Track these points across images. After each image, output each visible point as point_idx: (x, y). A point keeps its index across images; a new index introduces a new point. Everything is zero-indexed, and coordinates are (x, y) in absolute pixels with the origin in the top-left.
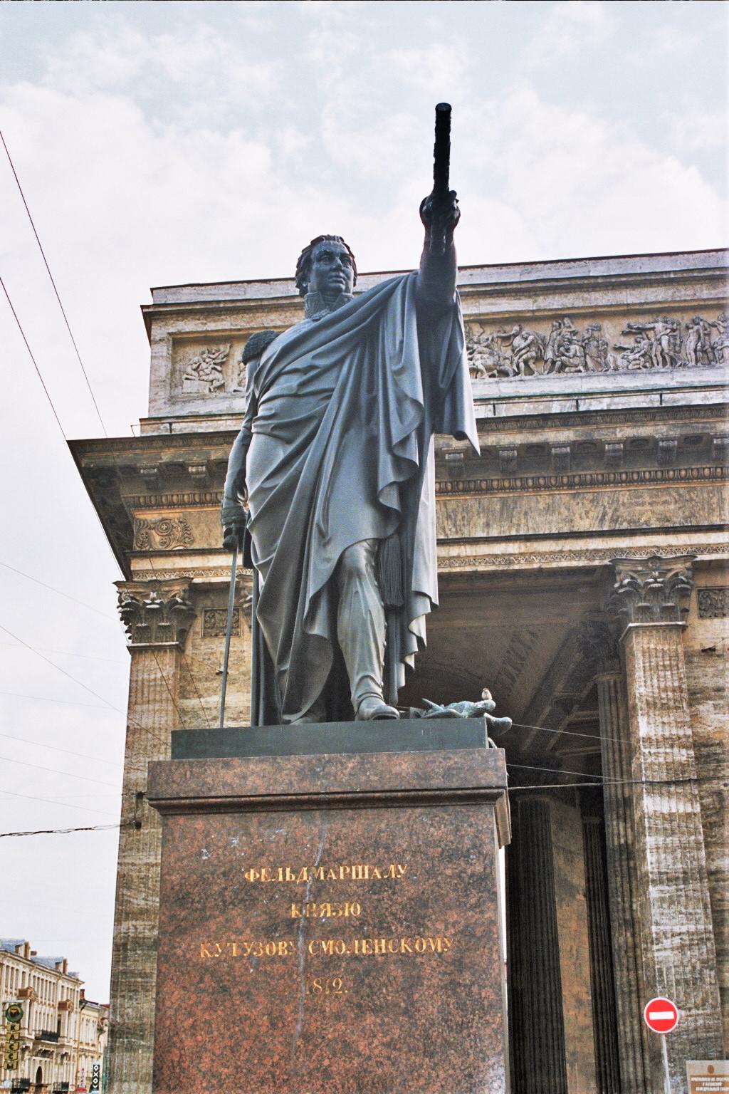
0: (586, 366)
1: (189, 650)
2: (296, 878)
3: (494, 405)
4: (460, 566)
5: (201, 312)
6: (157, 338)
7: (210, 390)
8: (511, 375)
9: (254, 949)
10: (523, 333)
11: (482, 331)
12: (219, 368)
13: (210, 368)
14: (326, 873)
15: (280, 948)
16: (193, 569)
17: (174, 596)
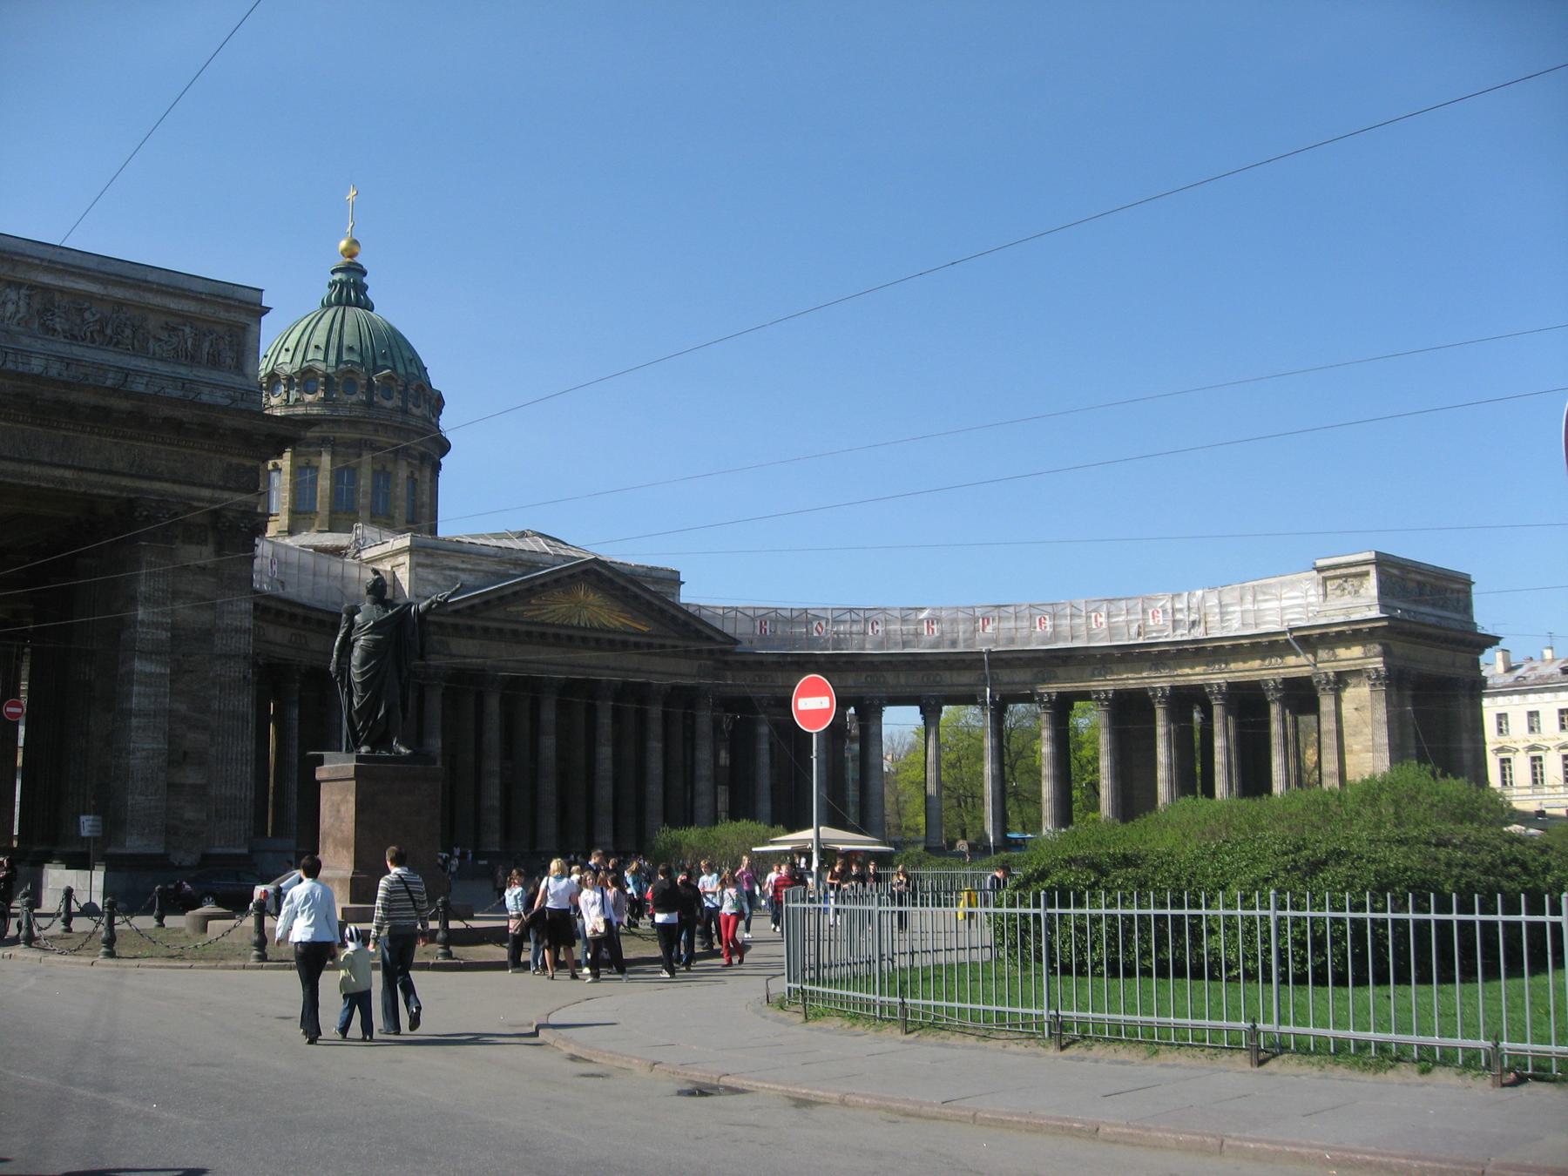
0: (133, 345)
3: (68, 364)
8: (79, 338)
10: (93, 310)
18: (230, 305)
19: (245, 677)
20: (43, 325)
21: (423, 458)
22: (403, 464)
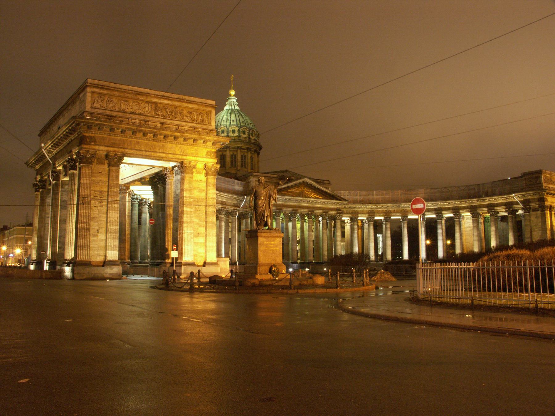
5: (100, 87)
6: (89, 91)
18: (206, 106)
19: (214, 212)
20: (156, 113)
21: (255, 151)
22: (249, 153)
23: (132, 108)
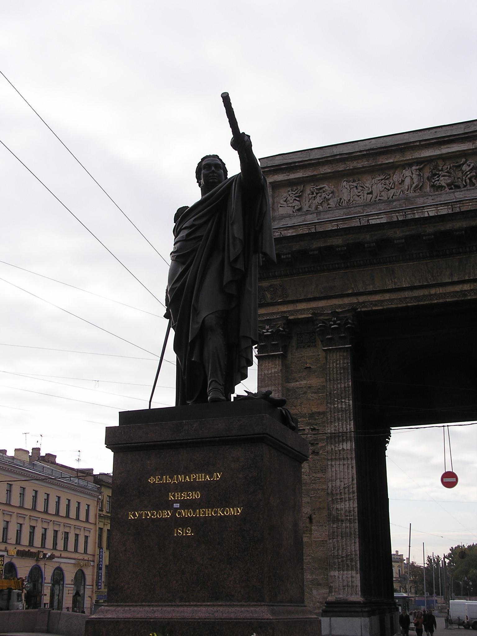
1: (290, 356)
2: (172, 481)
4: (437, 300)
7: (293, 212)
8: (462, 186)
9: (153, 514)
10: (468, 163)
11: (444, 163)
12: (298, 199)
13: (293, 199)
14: (185, 478)
15: (164, 515)
16: (289, 311)
17: (279, 327)
20: (433, 186)
23: (371, 193)
